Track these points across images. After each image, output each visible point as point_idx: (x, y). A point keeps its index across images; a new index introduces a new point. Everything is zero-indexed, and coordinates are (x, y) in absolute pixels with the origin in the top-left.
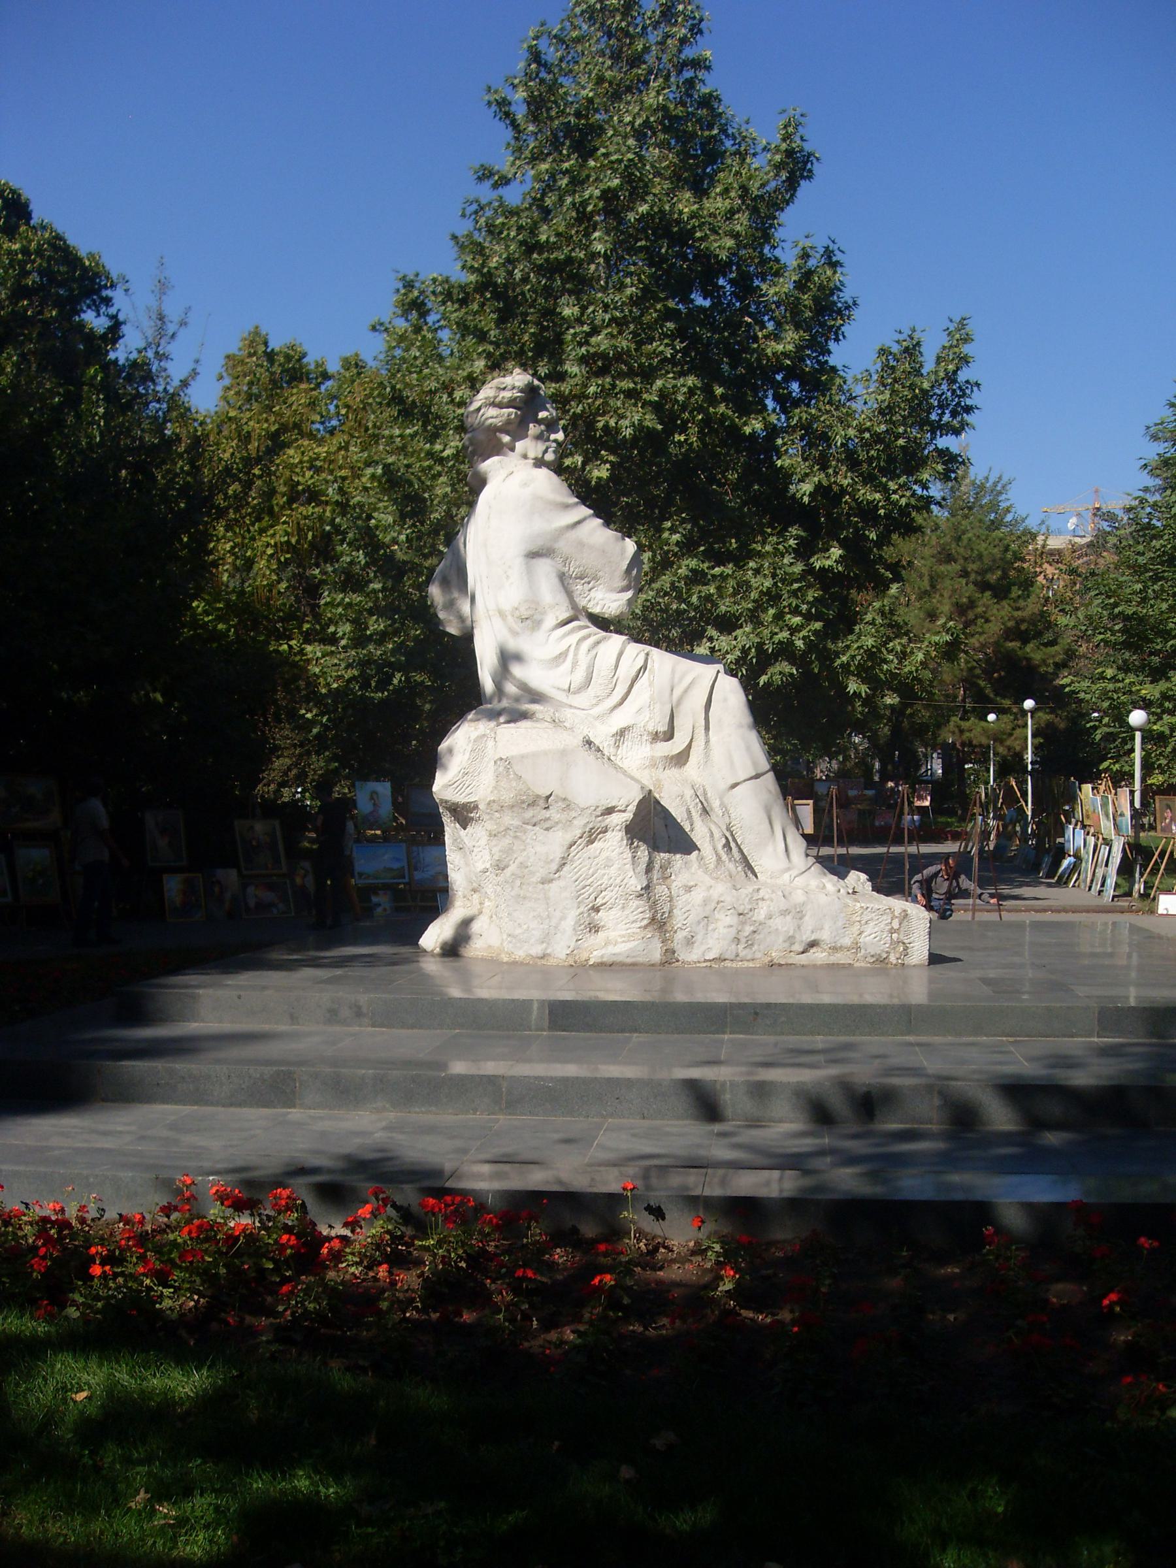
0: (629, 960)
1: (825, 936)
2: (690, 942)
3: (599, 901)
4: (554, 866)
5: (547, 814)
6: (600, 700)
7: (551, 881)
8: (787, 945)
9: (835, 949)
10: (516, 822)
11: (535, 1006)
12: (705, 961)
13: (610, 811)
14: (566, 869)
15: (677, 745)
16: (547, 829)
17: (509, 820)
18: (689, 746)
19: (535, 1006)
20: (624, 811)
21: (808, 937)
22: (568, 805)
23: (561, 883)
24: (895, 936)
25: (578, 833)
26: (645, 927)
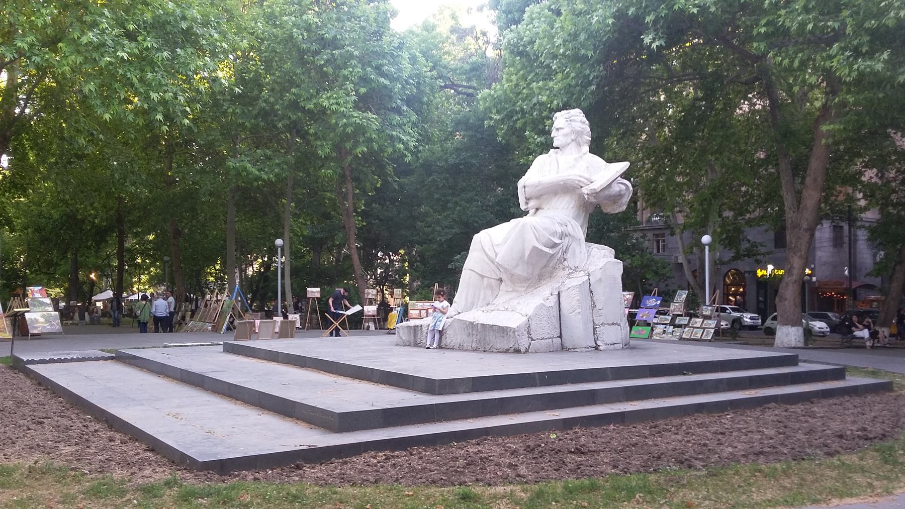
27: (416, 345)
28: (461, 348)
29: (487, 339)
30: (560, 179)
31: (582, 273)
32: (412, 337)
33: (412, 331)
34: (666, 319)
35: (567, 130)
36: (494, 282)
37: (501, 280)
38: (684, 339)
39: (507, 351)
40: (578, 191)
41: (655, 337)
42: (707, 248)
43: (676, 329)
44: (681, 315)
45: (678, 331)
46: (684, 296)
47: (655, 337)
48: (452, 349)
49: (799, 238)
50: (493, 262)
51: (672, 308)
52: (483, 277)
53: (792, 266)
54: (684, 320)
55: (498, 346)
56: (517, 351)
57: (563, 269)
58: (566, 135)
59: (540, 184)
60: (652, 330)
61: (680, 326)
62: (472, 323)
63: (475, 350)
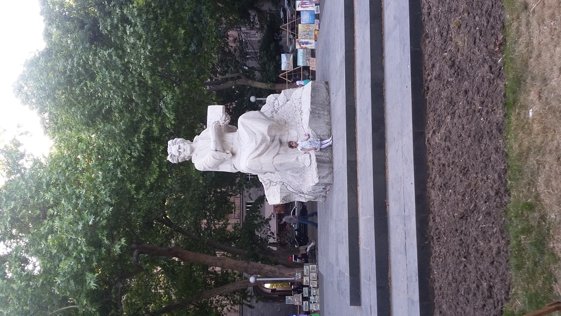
27: (331, 162)
28: (329, 124)
29: (321, 102)
30: (214, 131)
31: (276, 102)
32: (326, 165)
33: (322, 165)
34: (306, 305)
35: (181, 145)
36: (282, 148)
37: (281, 143)
38: (318, 285)
39: (328, 90)
40: (223, 130)
41: (318, 308)
42: (258, 279)
43: (312, 293)
44: (303, 295)
45: (313, 292)
46: (289, 298)
47: (318, 308)
48: (330, 130)
49: (253, 267)
50: (268, 147)
51: (297, 303)
52: (278, 154)
53: (269, 271)
54: (305, 290)
55: (325, 95)
56: (327, 83)
57: (273, 117)
58: (185, 145)
59: (215, 141)
60: (315, 312)
61: (310, 293)
62: (311, 113)
63: (329, 112)
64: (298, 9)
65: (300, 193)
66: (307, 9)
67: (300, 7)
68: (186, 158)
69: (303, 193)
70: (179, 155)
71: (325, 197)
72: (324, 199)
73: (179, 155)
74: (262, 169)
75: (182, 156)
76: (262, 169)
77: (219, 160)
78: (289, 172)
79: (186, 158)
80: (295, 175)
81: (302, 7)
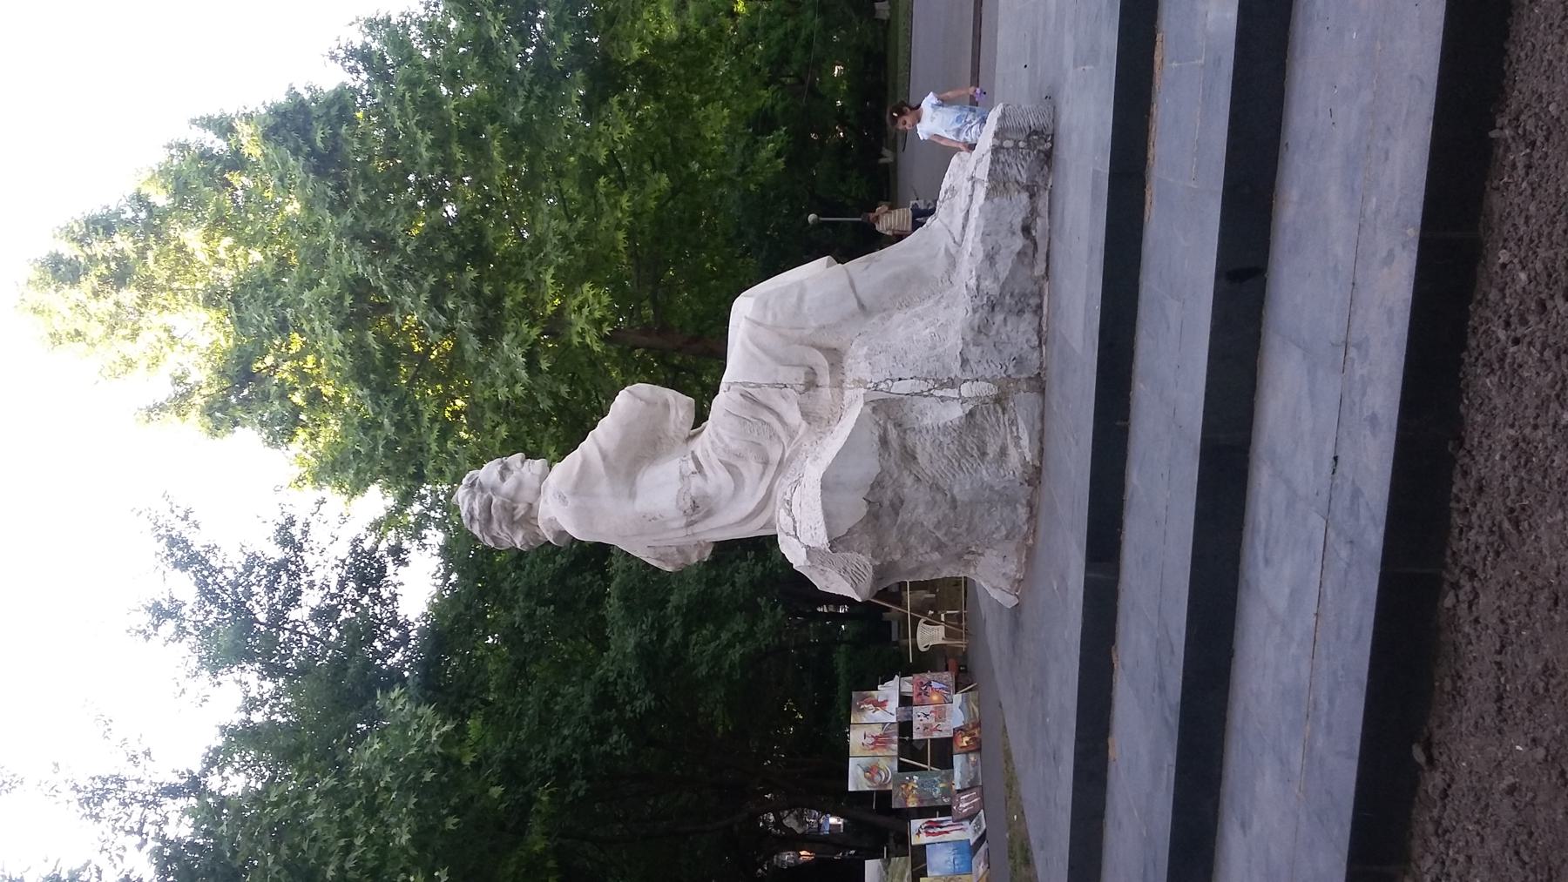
0: (1038, 426)
1: (1018, 222)
2: (1019, 362)
3: (975, 453)
4: (939, 497)
5: (886, 503)
6: (773, 435)
7: (954, 500)
8: (1026, 261)
9: (1034, 212)
10: (894, 531)
11: (1092, 575)
12: (1040, 345)
13: (884, 441)
14: (941, 483)
15: (821, 361)
16: (902, 502)
17: (892, 538)
18: (820, 348)
19: (1092, 575)
20: (885, 430)
21: (1019, 242)
22: (878, 484)
23: (956, 490)
24: (1021, 144)
25: (906, 473)
26: (1004, 410)
64: (915, 841)
65: (942, 386)
66: (946, 837)
67: (923, 835)
68: (521, 510)
69: (953, 383)
70: (503, 479)
71: (1039, 384)
72: (1033, 397)
73: (503, 479)
74: (801, 299)
75: (508, 486)
76: (801, 299)
77: (648, 403)
78: (898, 317)
79: (521, 510)
80: (919, 309)
81: (928, 834)
